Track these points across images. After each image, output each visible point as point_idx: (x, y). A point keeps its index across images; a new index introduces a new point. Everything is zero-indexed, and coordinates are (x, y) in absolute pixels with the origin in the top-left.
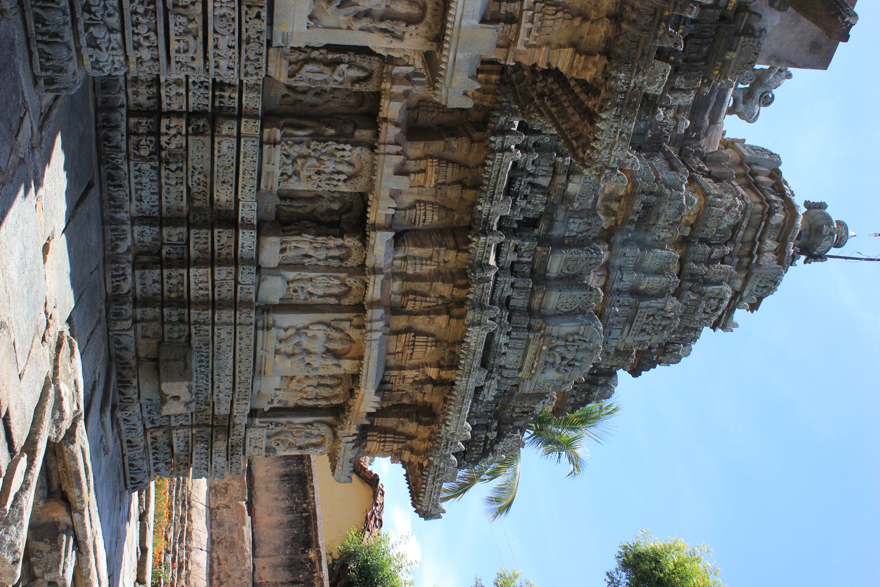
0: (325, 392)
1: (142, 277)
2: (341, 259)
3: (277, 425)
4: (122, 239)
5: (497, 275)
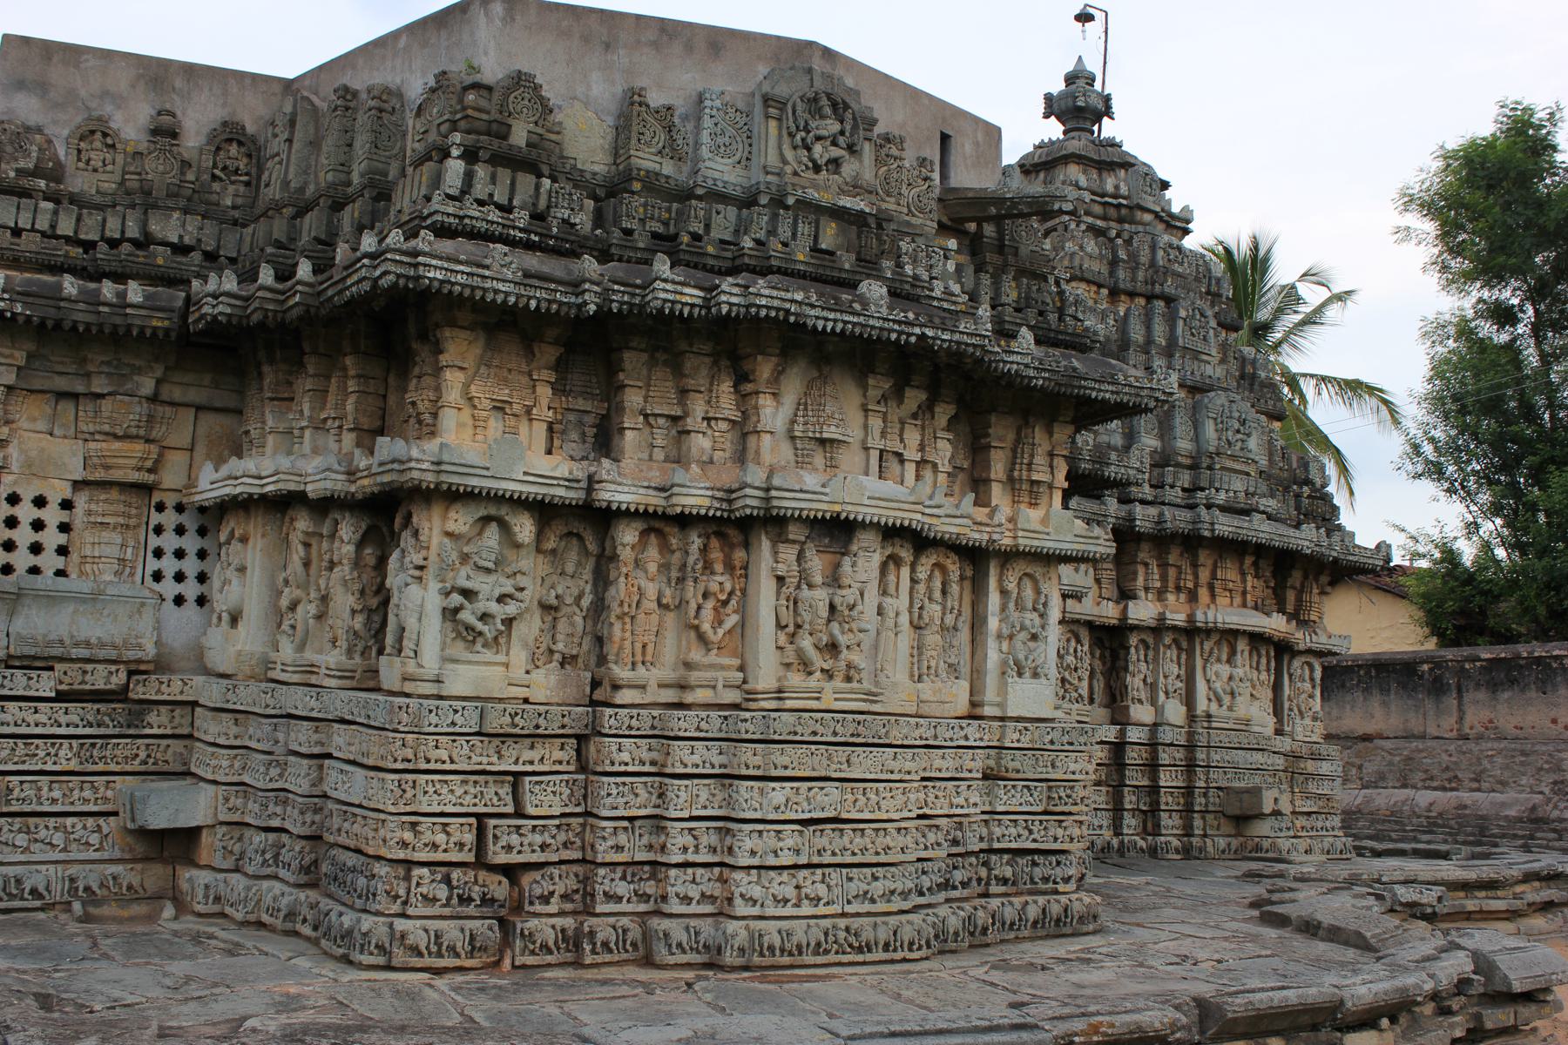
0: (1263, 666)
1: (1166, 828)
2: (1147, 647)
3: (1291, 710)
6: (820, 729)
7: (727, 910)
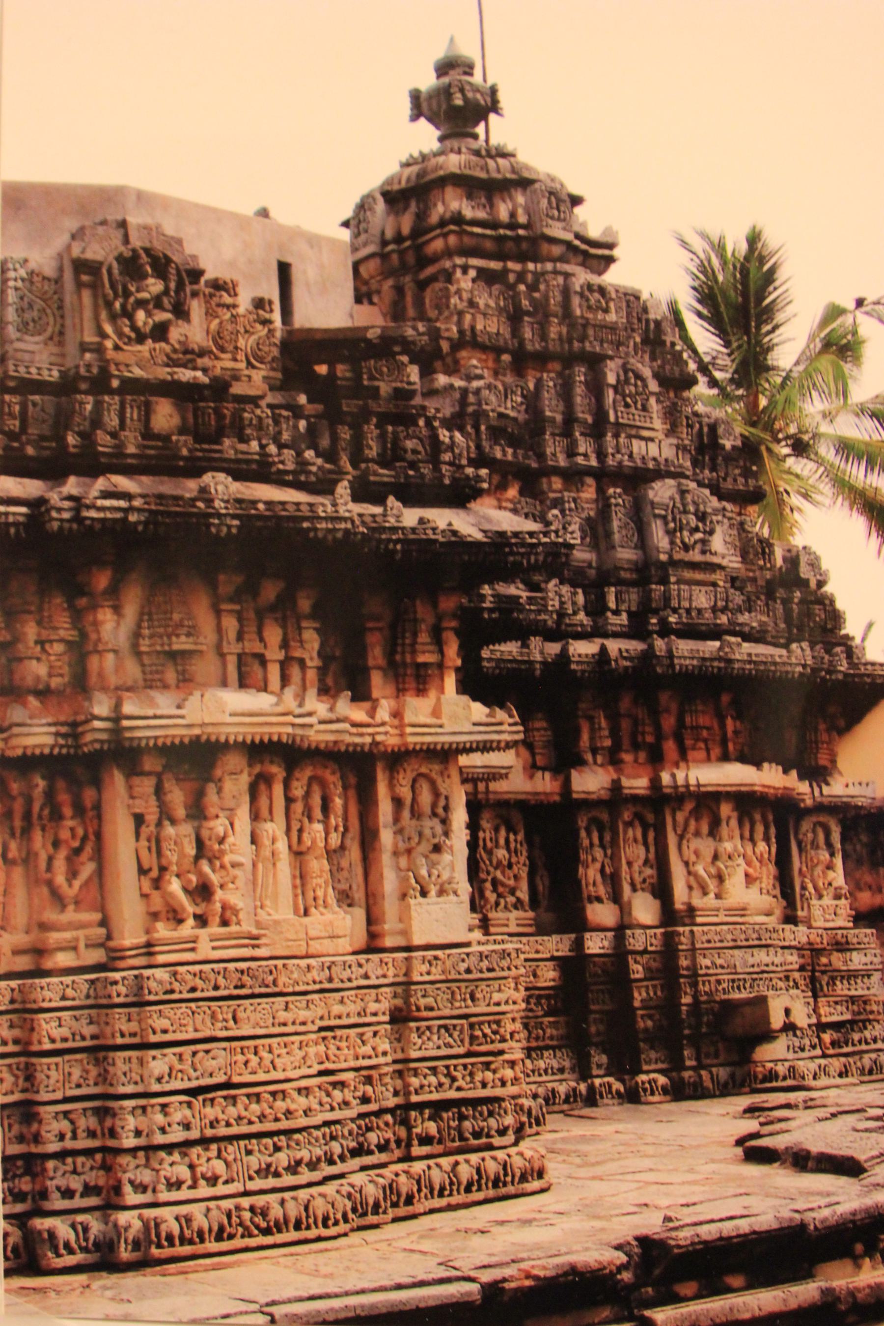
1: (649, 1062)
3: (804, 888)
4: (610, 1086)
5: (606, 635)
7: (115, 1200)
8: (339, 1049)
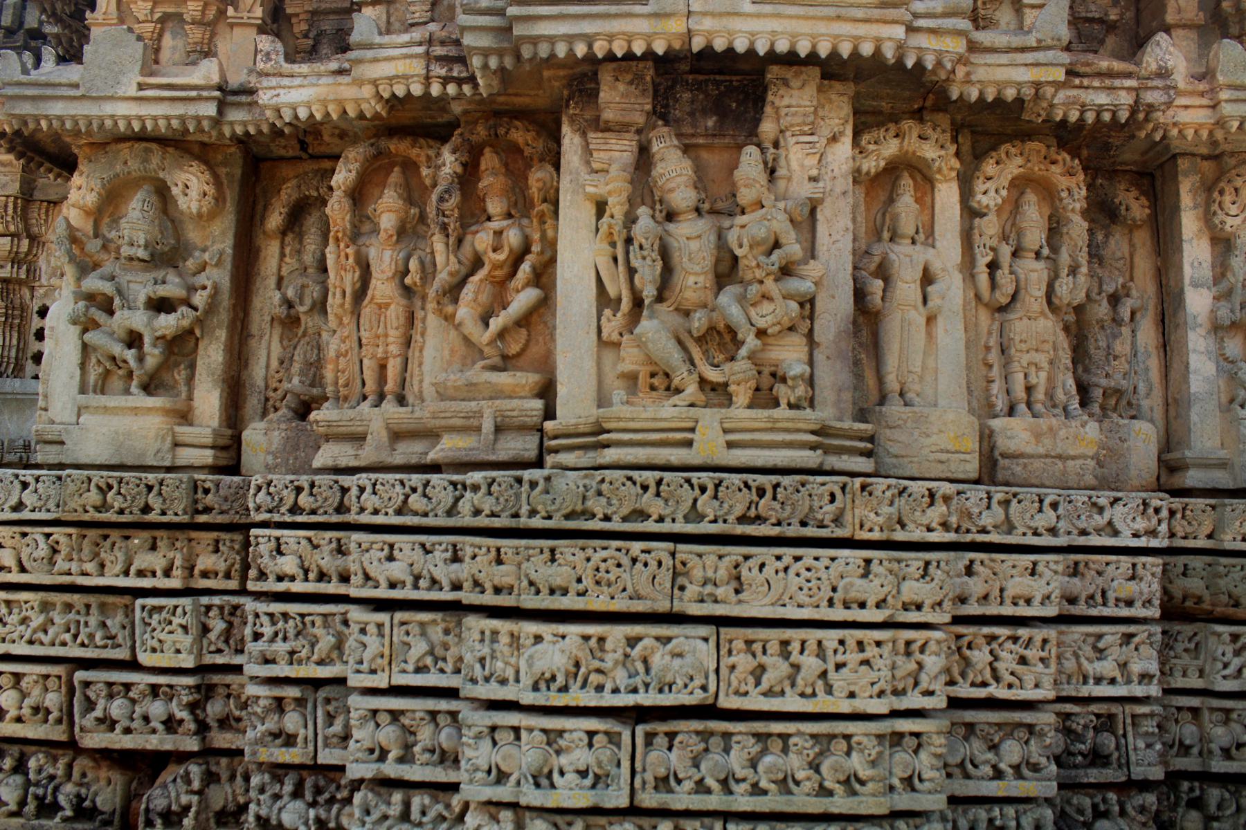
6: (656, 507)
8: (1023, 661)
